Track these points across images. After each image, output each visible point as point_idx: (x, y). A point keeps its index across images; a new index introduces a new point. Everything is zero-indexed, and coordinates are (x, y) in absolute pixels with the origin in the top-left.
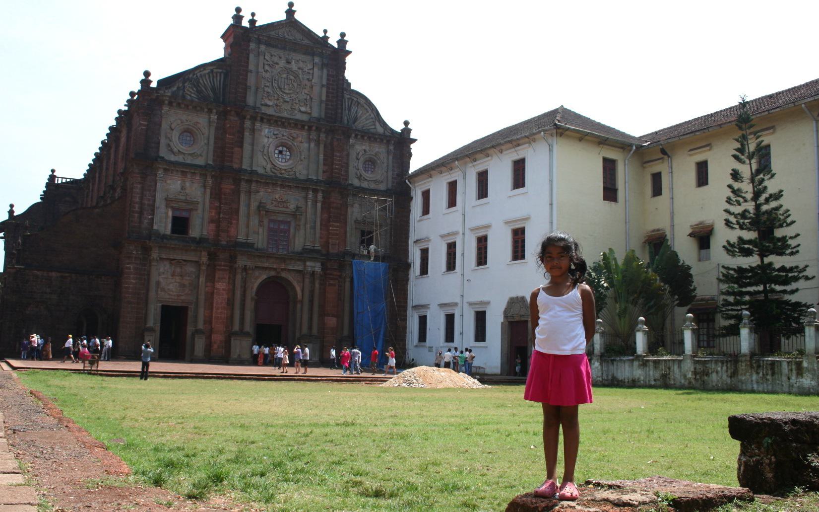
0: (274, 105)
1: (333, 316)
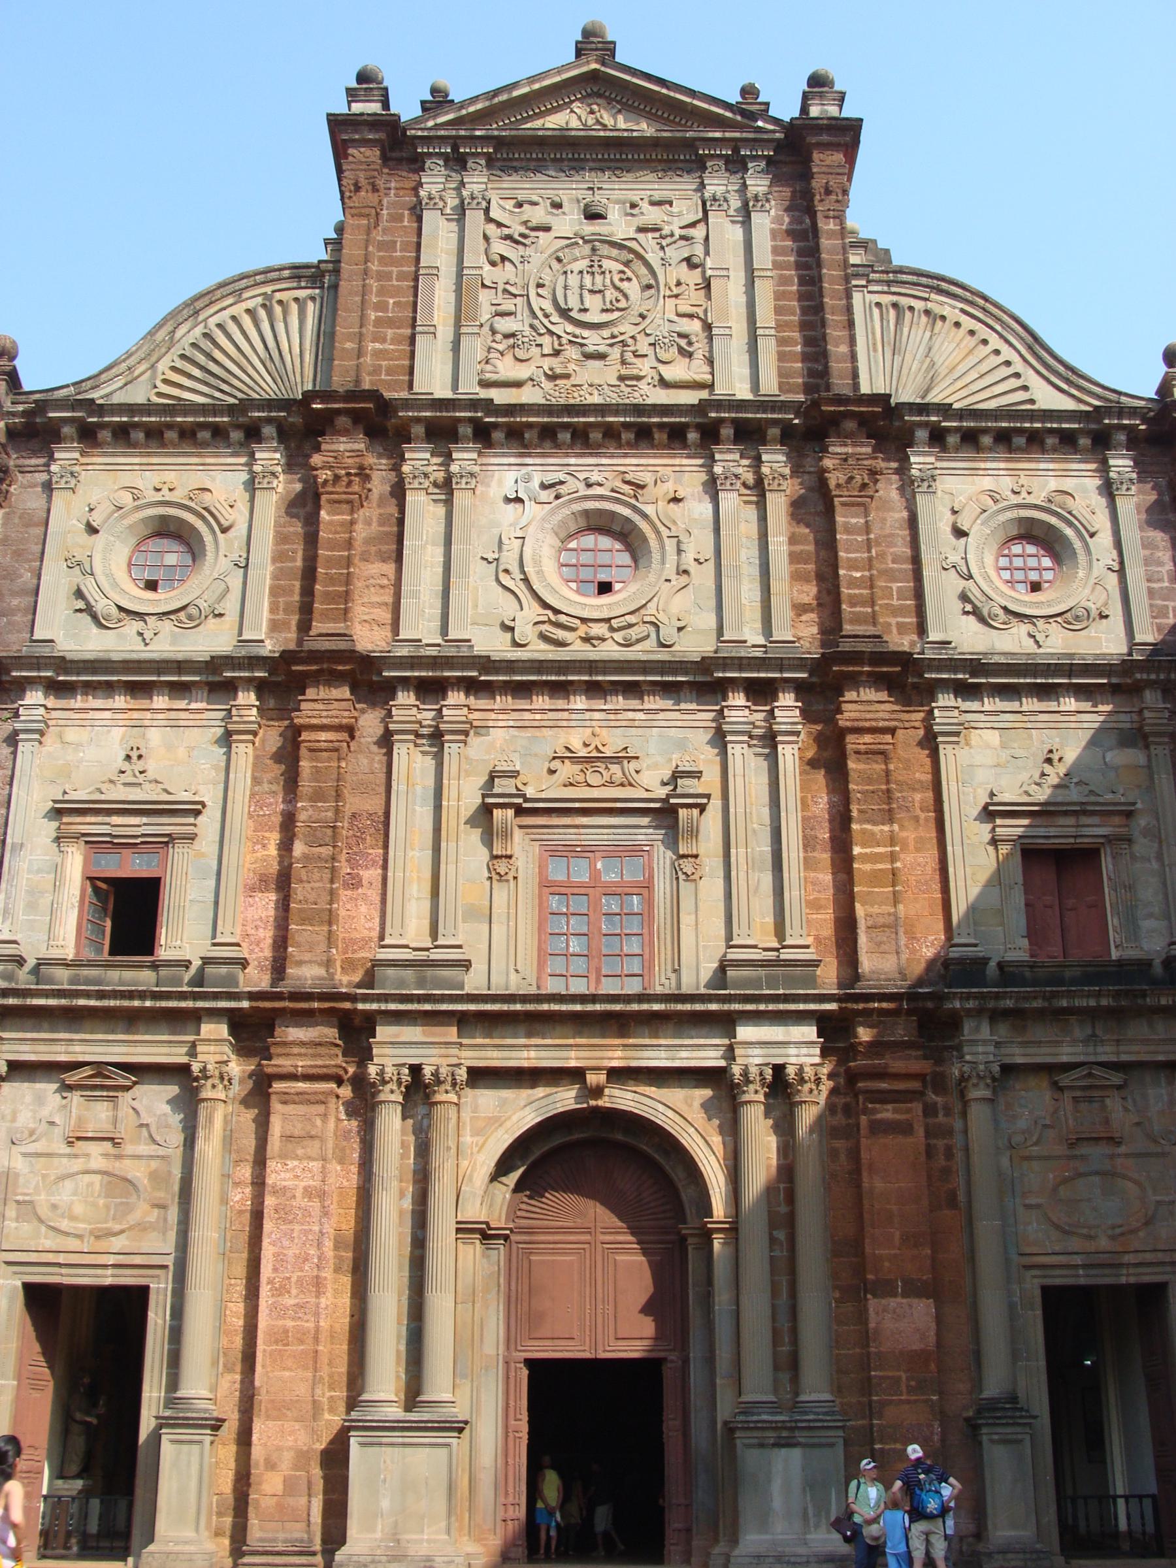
1: (913, 1290)
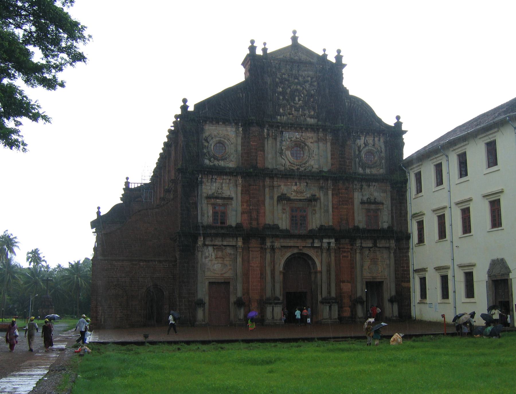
1: (348, 282)
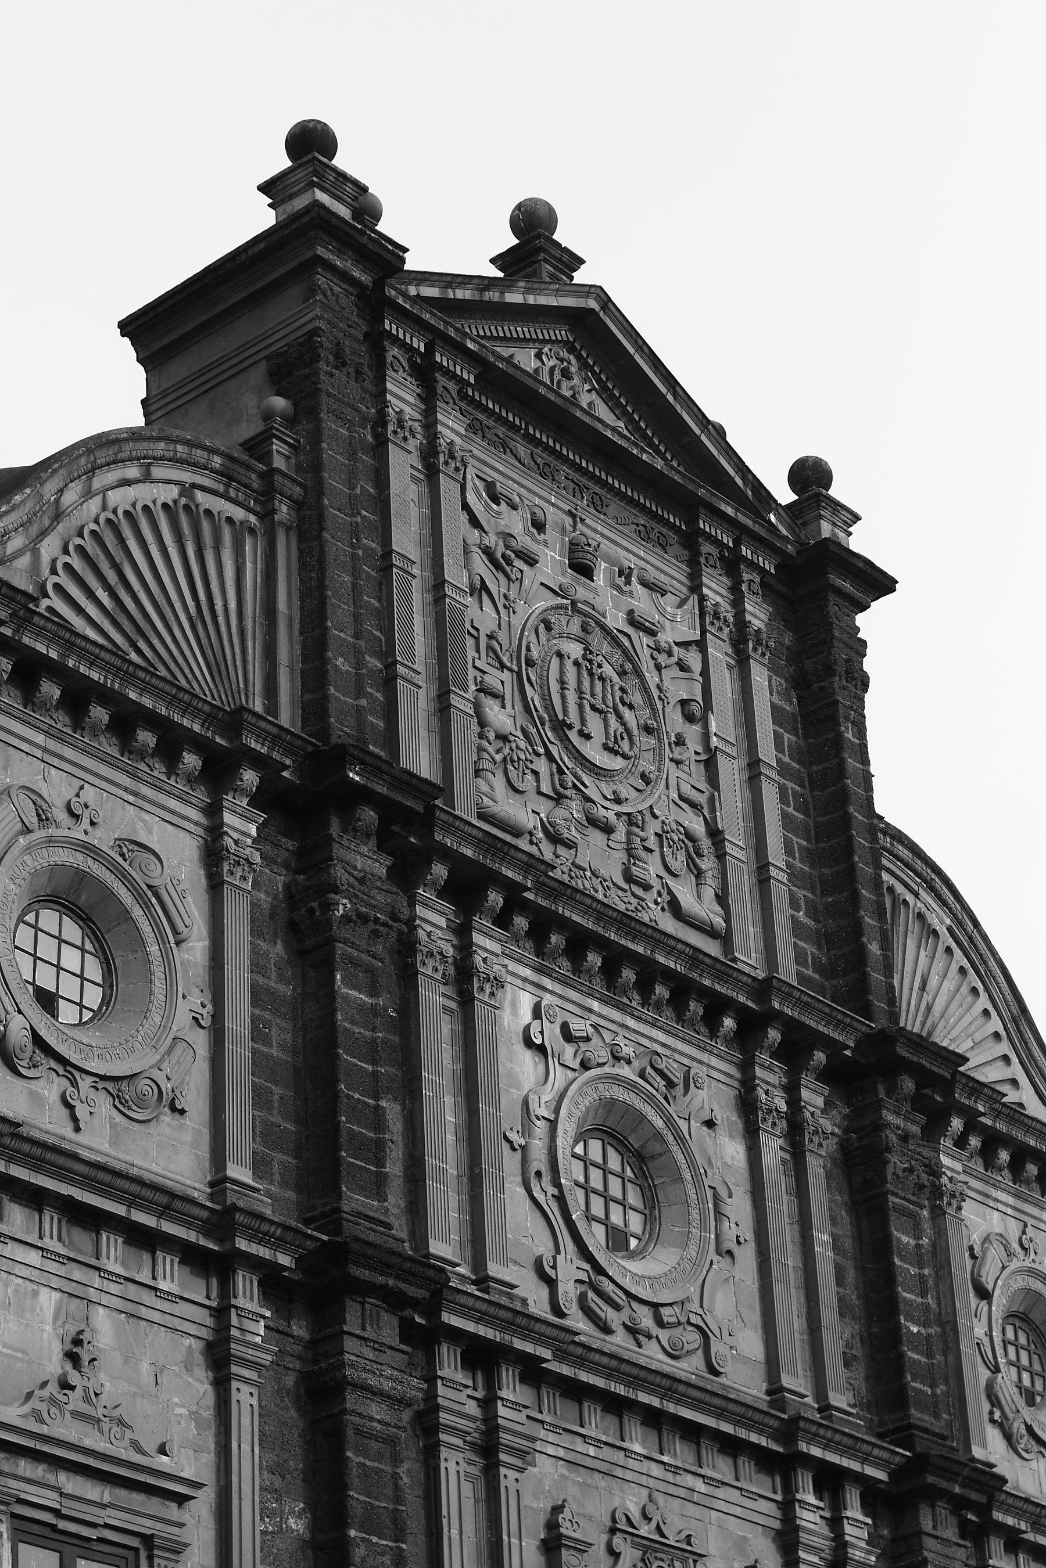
0: (541, 835)
